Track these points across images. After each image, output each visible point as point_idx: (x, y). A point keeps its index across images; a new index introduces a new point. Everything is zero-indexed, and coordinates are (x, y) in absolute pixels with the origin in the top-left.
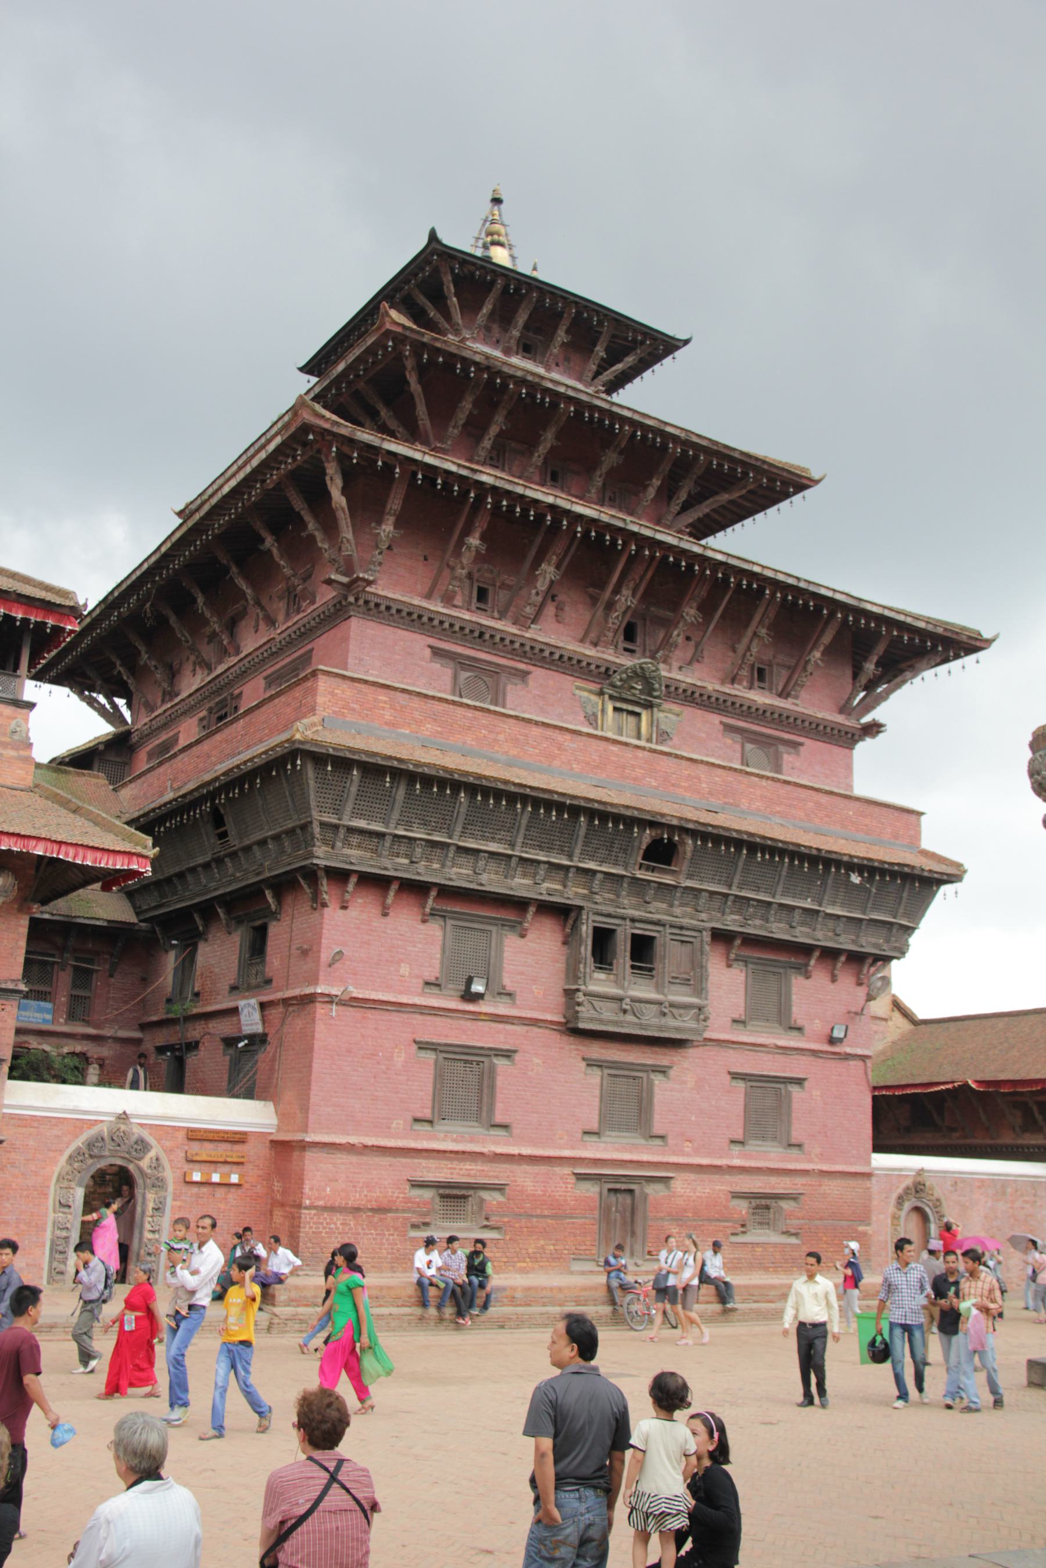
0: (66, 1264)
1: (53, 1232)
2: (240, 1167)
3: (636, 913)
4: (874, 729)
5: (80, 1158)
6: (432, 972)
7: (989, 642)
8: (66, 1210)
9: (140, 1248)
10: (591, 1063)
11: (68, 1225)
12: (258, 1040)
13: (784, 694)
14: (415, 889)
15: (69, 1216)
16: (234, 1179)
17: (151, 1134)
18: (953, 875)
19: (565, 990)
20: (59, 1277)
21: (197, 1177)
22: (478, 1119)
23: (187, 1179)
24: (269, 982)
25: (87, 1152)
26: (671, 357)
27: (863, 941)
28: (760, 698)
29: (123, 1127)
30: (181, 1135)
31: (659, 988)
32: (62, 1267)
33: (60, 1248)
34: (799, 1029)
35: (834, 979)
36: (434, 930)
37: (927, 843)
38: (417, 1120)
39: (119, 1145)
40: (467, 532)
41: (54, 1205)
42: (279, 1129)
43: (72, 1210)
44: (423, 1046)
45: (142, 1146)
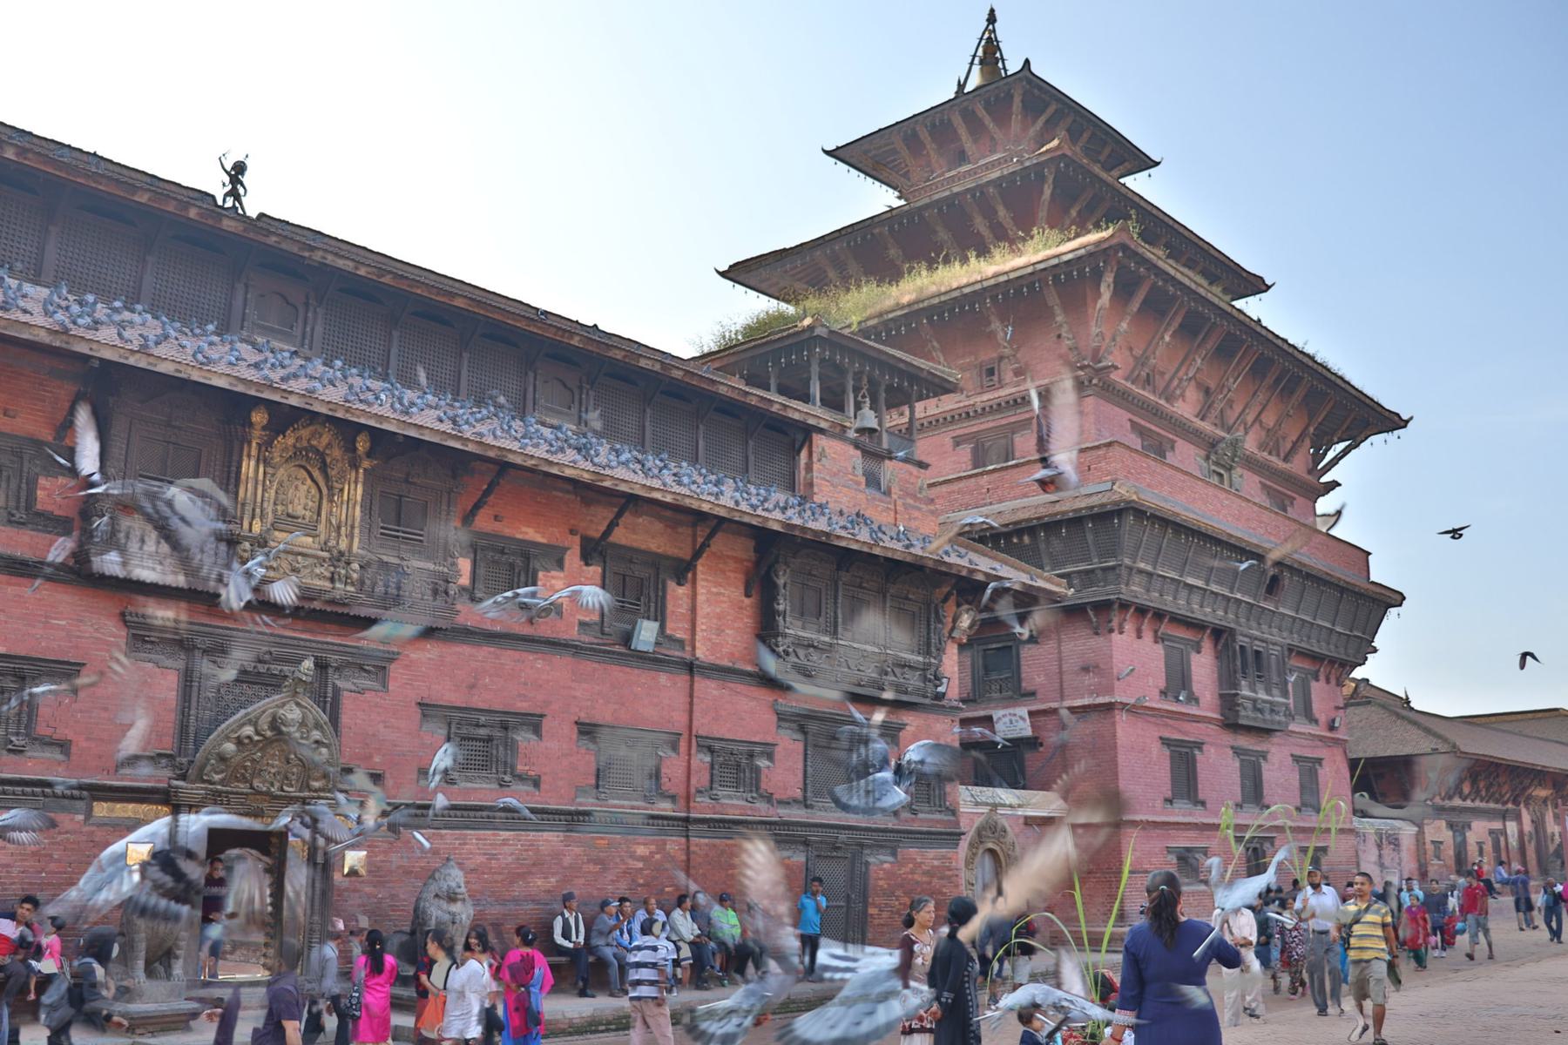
3: (1257, 633)
6: (1162, 684)
7: (1404, 424)
10: (1237, 751)
12: (1033, 743)
13: (1286, 459)
14: (1159, 615)
18: (1397, 599)
19: (1221, 696)
22: (1189, 798)
24: (1033, 694)
26: (1146, 173)
27: (1350, 651)
28: (1281, 465)
30: (1021, 821)
31: (1268, 692)
34: (1316, 722)
35: (1328, 681)
36: (1159, 650)
37: (1372, 578)
38: (1166, 800)
40: (1166, 330)
44: (1165, 742)
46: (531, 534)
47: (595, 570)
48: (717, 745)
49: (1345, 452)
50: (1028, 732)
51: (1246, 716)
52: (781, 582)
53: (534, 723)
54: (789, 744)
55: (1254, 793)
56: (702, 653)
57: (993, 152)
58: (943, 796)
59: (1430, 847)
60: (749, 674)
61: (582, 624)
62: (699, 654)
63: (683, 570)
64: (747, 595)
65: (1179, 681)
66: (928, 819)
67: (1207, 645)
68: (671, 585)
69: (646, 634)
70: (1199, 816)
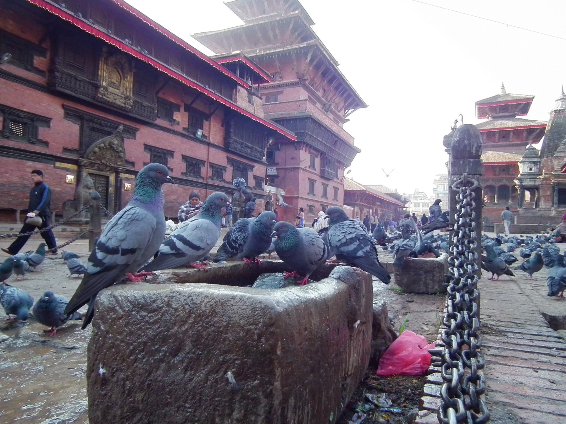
4: (349, 120)
12: (277, 176)
13: (339, 112)
14: (311, 147)
24: (278, 164)
42: (286, 194)
45: (271, 198)
46: (172, 100)
47: (187, 114)
48: (214, 166)
49: (352, 112)
50: (276, 174)
51: (326, 175)
52: (232, 123)
53: (171, 153)
54: (230, 169)
55: (325, 195)
56: (212, 140)
57: (273, 12)
58: (261, 186)
59: (355, 213)
60: (221, 147)
61: (183, 128)
62: (211, 140)
63: (208, 117)
64: (222, 126)
65: (313, 165)
66: (257, 191)
67: (319, 156)
68: (205, 121)
69: (200, 133)
70: (314, 198)
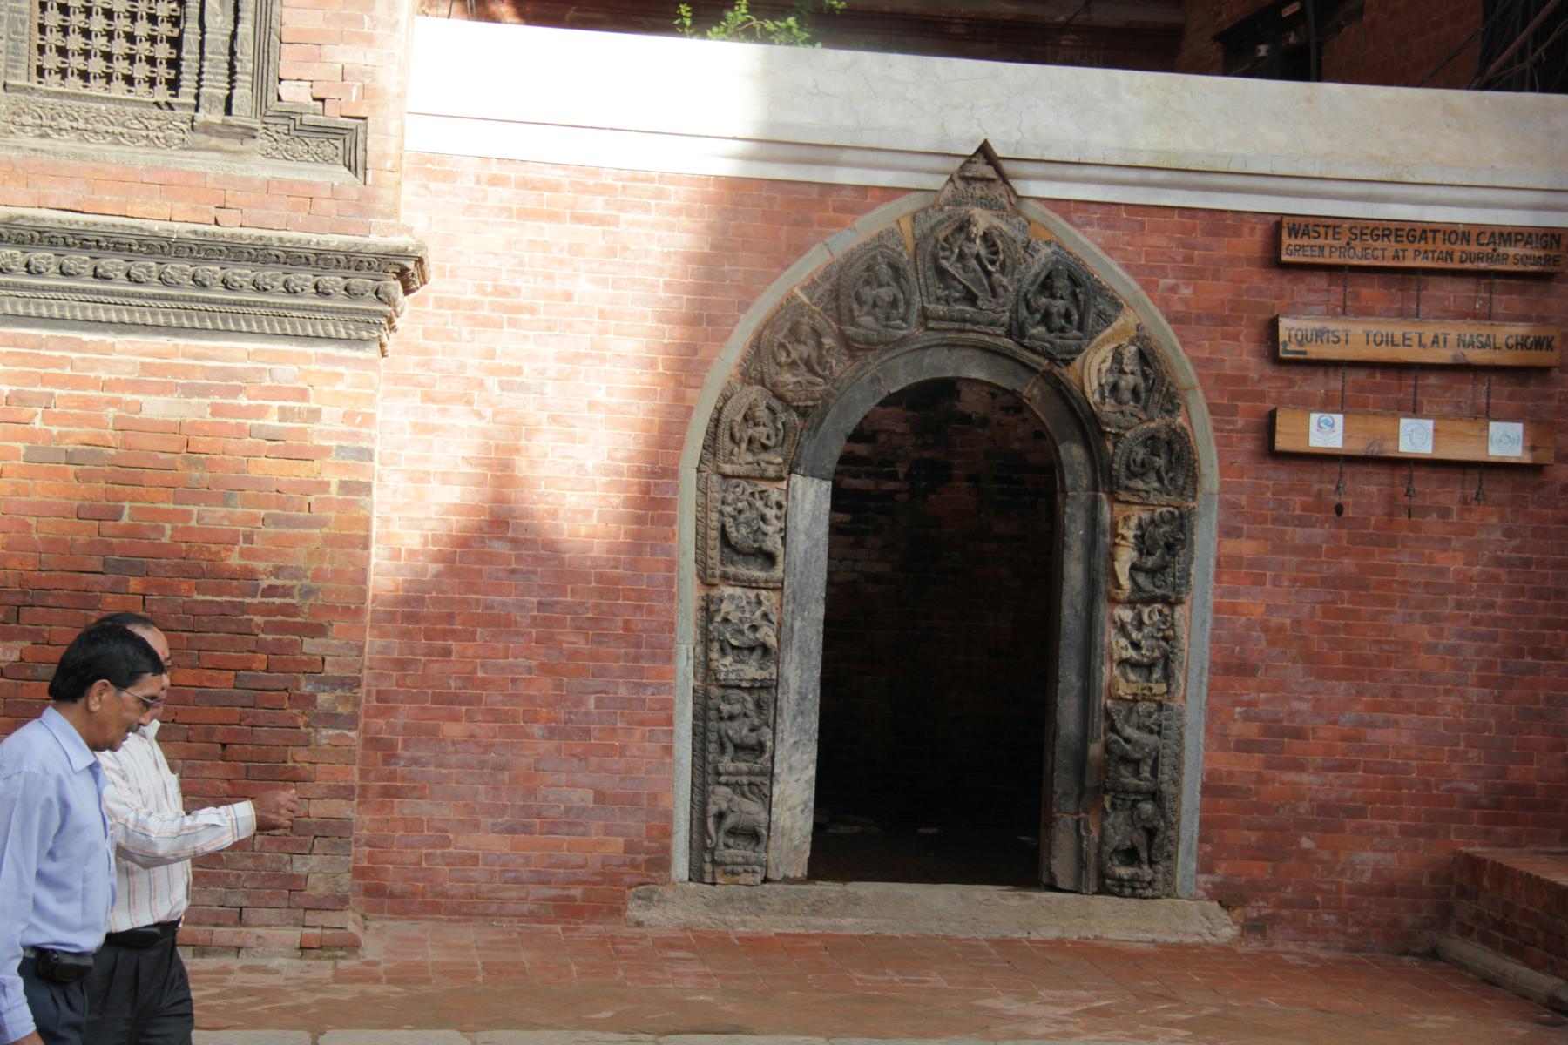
0: (767, 800)
1: (706, 669)
2: (1533, 387)
5: (806, 350)
8: (757, 573)
9: (1085, 738)
11: (767, 635)
15: (770, 599)
16: (1505, 441)
17: (1108, 250)
20: (739, 852)
21: (1326, 432)
23: (1282, 443)
25: (829, 326)
29: (983, 220)
32: (752, 809)
33: (739, 730)
39: (971, 298)
41: (702, 549)
43: (778, 572)
